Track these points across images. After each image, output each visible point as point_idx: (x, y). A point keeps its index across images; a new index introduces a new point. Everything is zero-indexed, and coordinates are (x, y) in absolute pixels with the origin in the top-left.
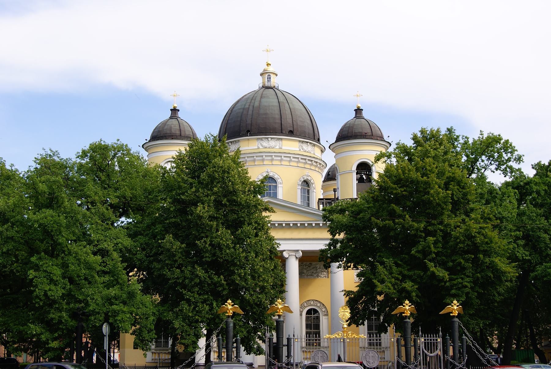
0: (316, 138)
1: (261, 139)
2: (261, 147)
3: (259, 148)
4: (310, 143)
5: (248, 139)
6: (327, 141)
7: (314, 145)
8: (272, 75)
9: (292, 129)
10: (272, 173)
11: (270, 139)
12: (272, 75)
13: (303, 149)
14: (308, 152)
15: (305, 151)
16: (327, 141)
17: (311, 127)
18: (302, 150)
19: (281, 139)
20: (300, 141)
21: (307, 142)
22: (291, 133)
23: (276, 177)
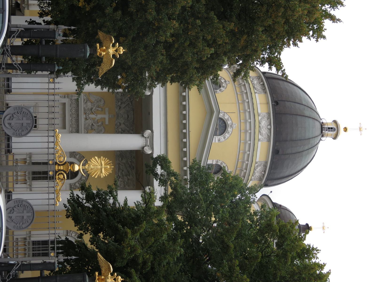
0: (268, 183)
1: (269, 118)
2: (260, 118)
3: (259, 115)
4: (264, 175)
5: (268, 103)
6: (271, 192)
7: (261, 179)
8: (335, 133)
9: (280, 152)
10: (231, 130)
11: (269, 127)
12: (335, 133)
13: (257, 166)
14: (254, 172)
15: (255, 169)
16: (271, 192)
17: (282, 175)
18: (256, 165)
19: (269, 140)
20: (266, 163)
21: (265, 172)
22: (276, 152)
23: (227, 135)
